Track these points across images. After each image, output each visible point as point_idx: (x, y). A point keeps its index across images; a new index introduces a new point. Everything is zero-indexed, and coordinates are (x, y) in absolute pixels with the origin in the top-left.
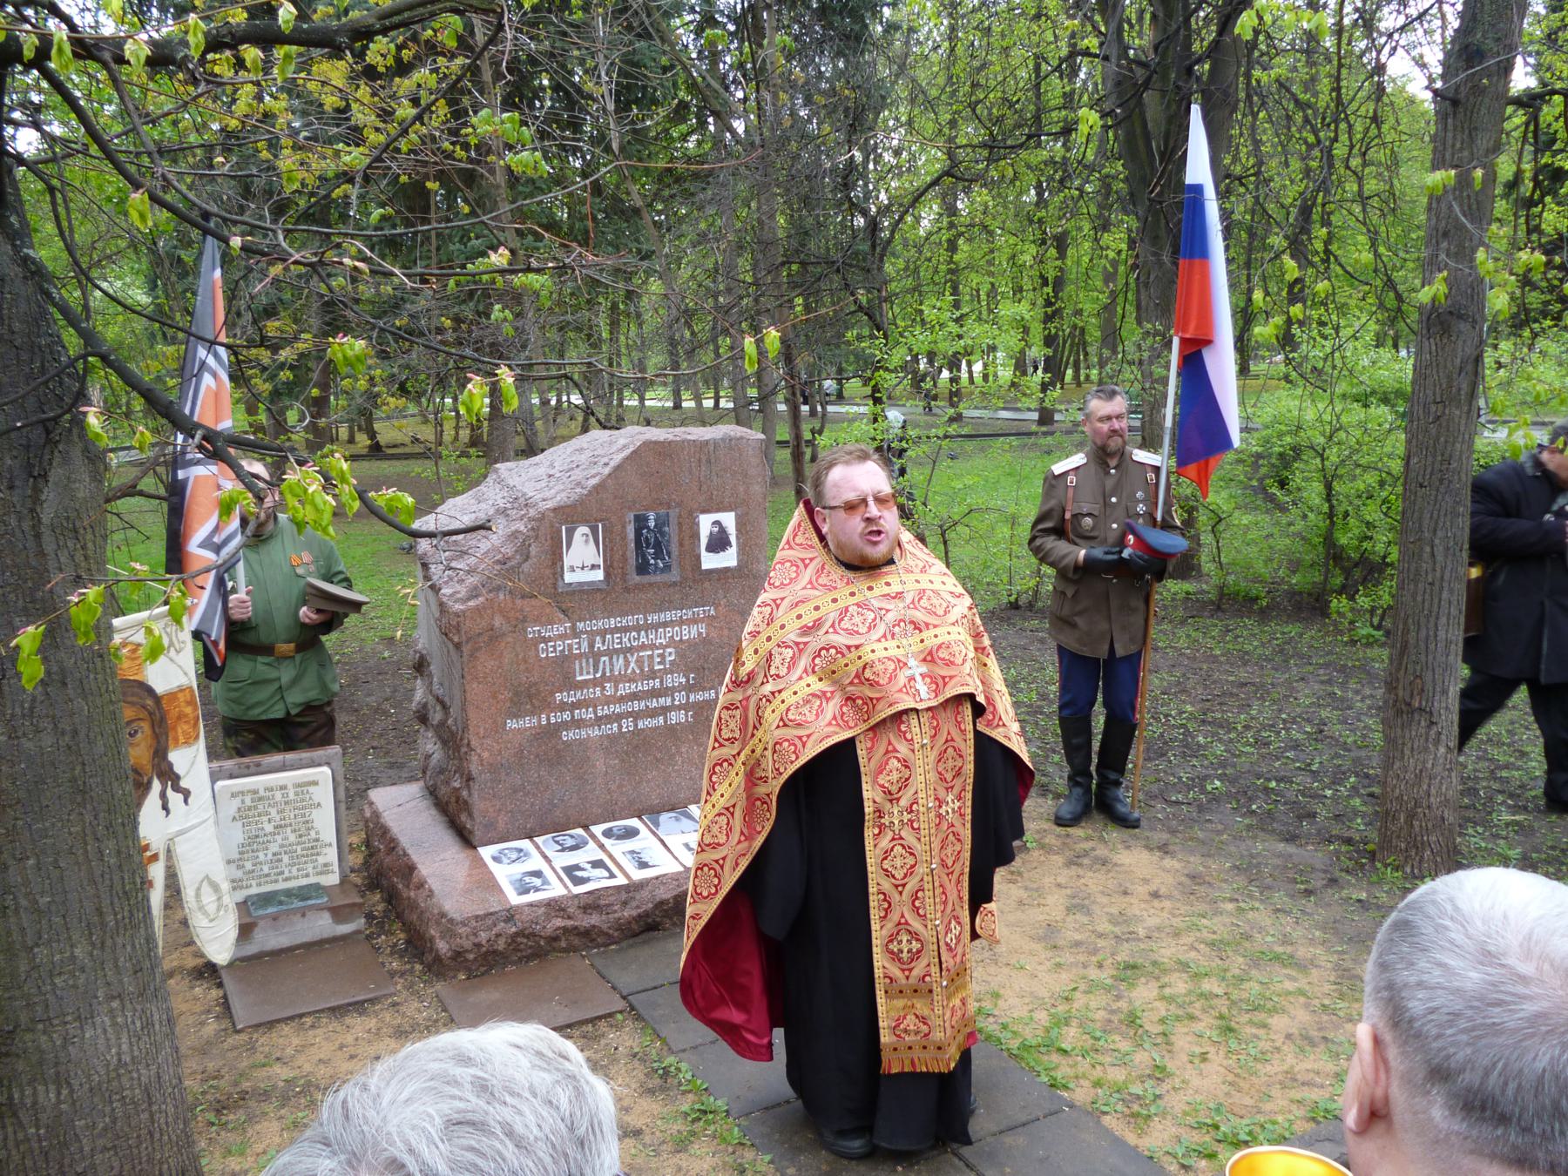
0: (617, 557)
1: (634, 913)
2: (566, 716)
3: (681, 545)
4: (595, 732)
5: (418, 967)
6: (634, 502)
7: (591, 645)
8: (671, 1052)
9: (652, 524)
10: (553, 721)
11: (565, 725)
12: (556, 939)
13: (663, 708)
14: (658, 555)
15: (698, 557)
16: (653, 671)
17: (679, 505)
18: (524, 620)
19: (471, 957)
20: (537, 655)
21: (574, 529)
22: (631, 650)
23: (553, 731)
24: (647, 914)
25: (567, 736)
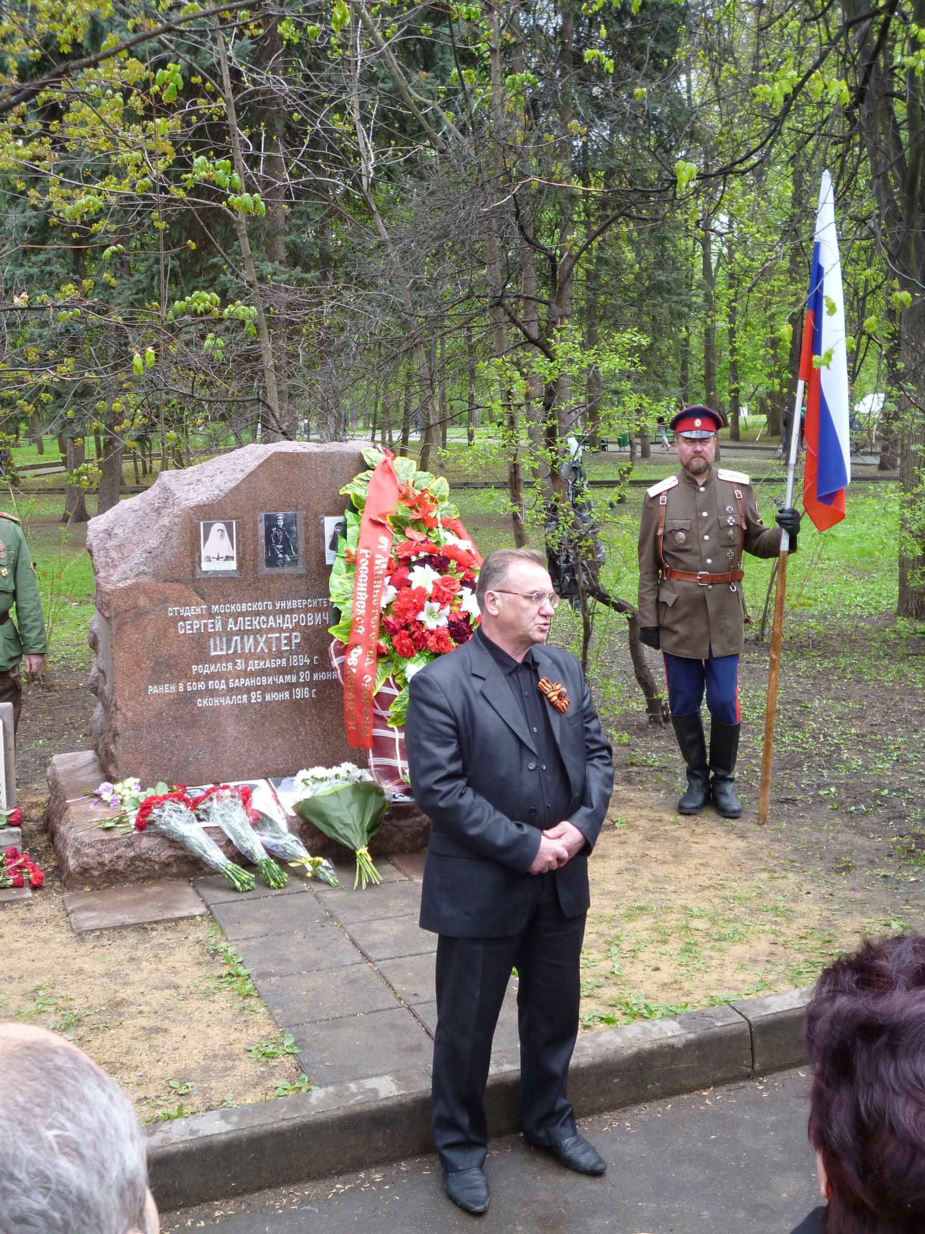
0: (249, 550)
2: (201, 686)
3: (307, 542)
4: (227, 701)
5: (57, 883)
6: (265, 504)
7: (225, 625)
8: (227, 940)
9: (281, 523)
12: (168, 865)
13: (288, 684)
14: (285, 551)
15: (323, 553)
16: (279, 651)
17: (306, 507)
18: (166, 601)
19: (96, 873)
20: (177, 632)
21: (211, 525)
22: (260, 631)
23: (188, 698)
25: (201, 703)
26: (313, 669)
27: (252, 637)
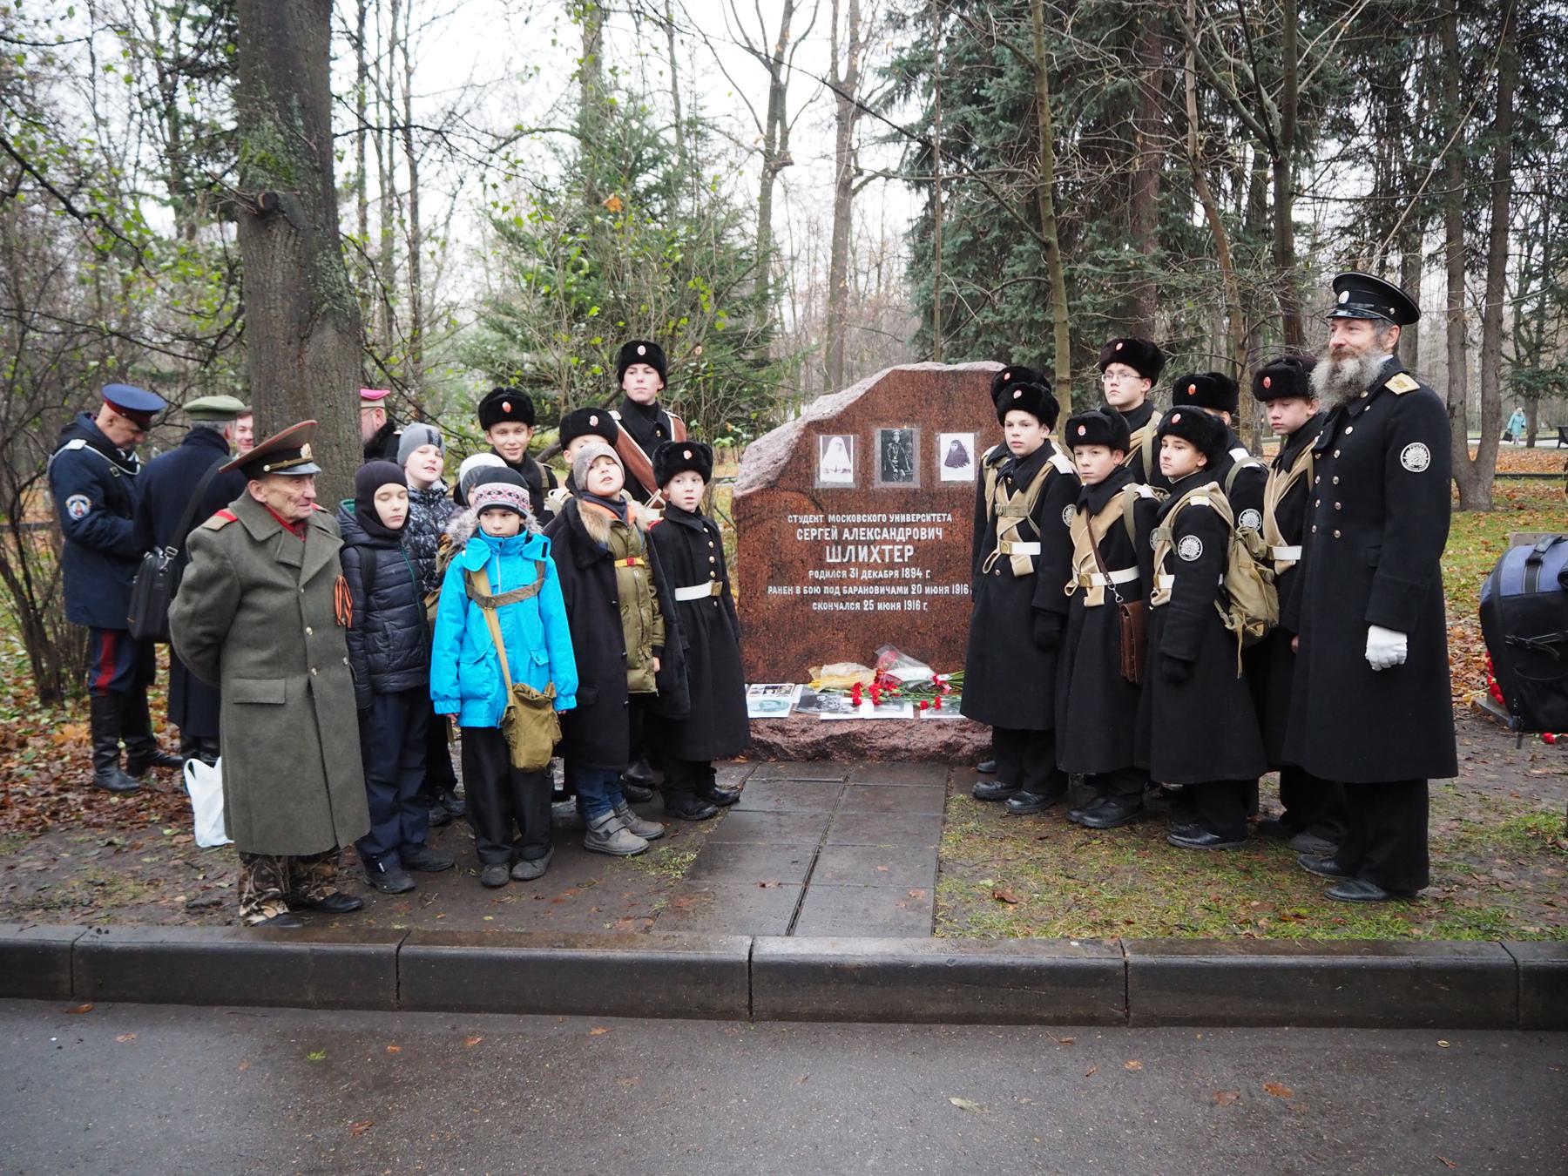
1: (808, 740)
2: (817, 590)
7: (840, 534)
9: (897, 439)
10: (805, 592)
11: (815, 598)
14: (901, 466)
22: (874, 542)
23: (807, 600)
24: (818, 743)
25: (818, 606)
26: (925, 582)
27: (866, 548)
